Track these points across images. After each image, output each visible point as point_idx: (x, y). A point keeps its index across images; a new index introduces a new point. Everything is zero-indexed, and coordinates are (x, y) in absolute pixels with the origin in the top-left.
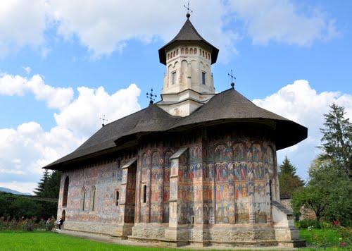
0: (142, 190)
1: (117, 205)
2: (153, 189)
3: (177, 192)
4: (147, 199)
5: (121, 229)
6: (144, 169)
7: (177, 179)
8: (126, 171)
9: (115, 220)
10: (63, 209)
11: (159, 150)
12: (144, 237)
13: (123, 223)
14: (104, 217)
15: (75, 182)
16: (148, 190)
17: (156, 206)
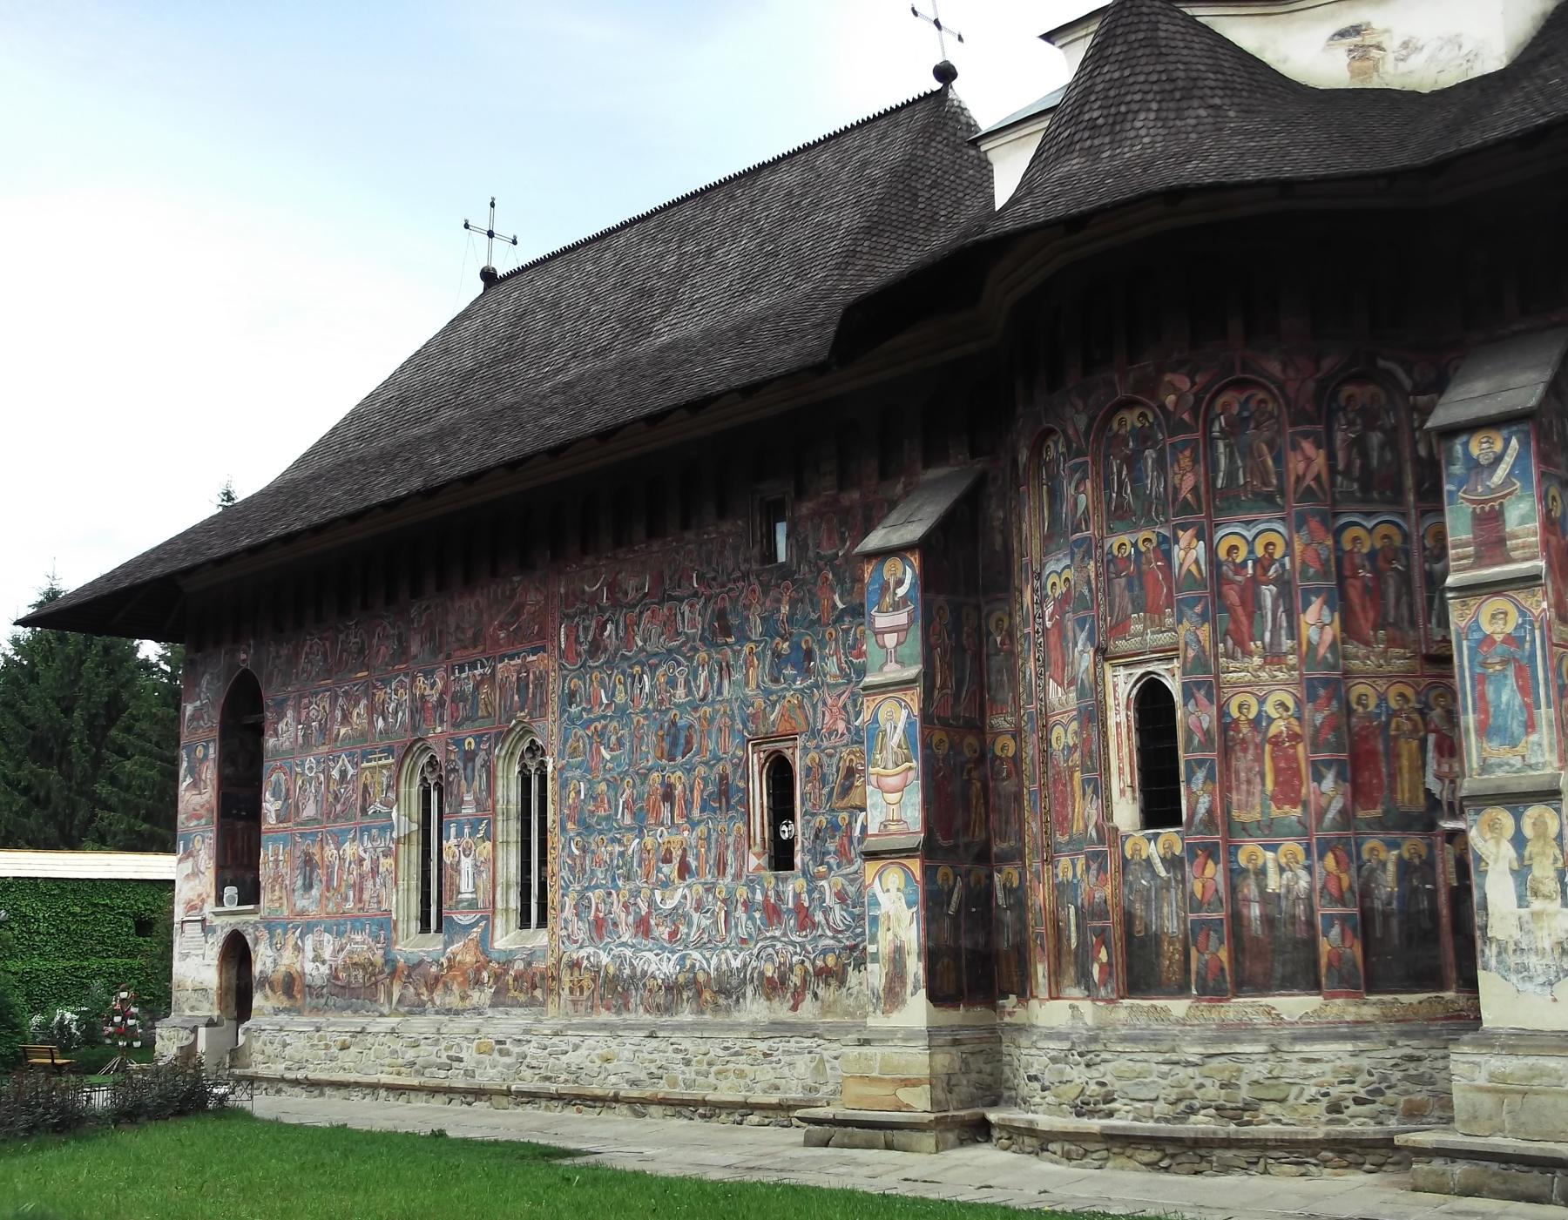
0: (1120, 717)
1: (781, 856)
2: (1242, 705)
3: (1545, 714)
4: (1196, 796)
5: (917, 1059)
6: (1122, 542)
7: (1540, 604)
8: (905, 576)
9: (773, 987)
10: (224, 926)
11: (1275, 368)
12: (1202, 1124)
13: (916, 1010)
14: (661, 966)
15: (317, 709)
16: (1191, 718)
17: (1292, 847)
